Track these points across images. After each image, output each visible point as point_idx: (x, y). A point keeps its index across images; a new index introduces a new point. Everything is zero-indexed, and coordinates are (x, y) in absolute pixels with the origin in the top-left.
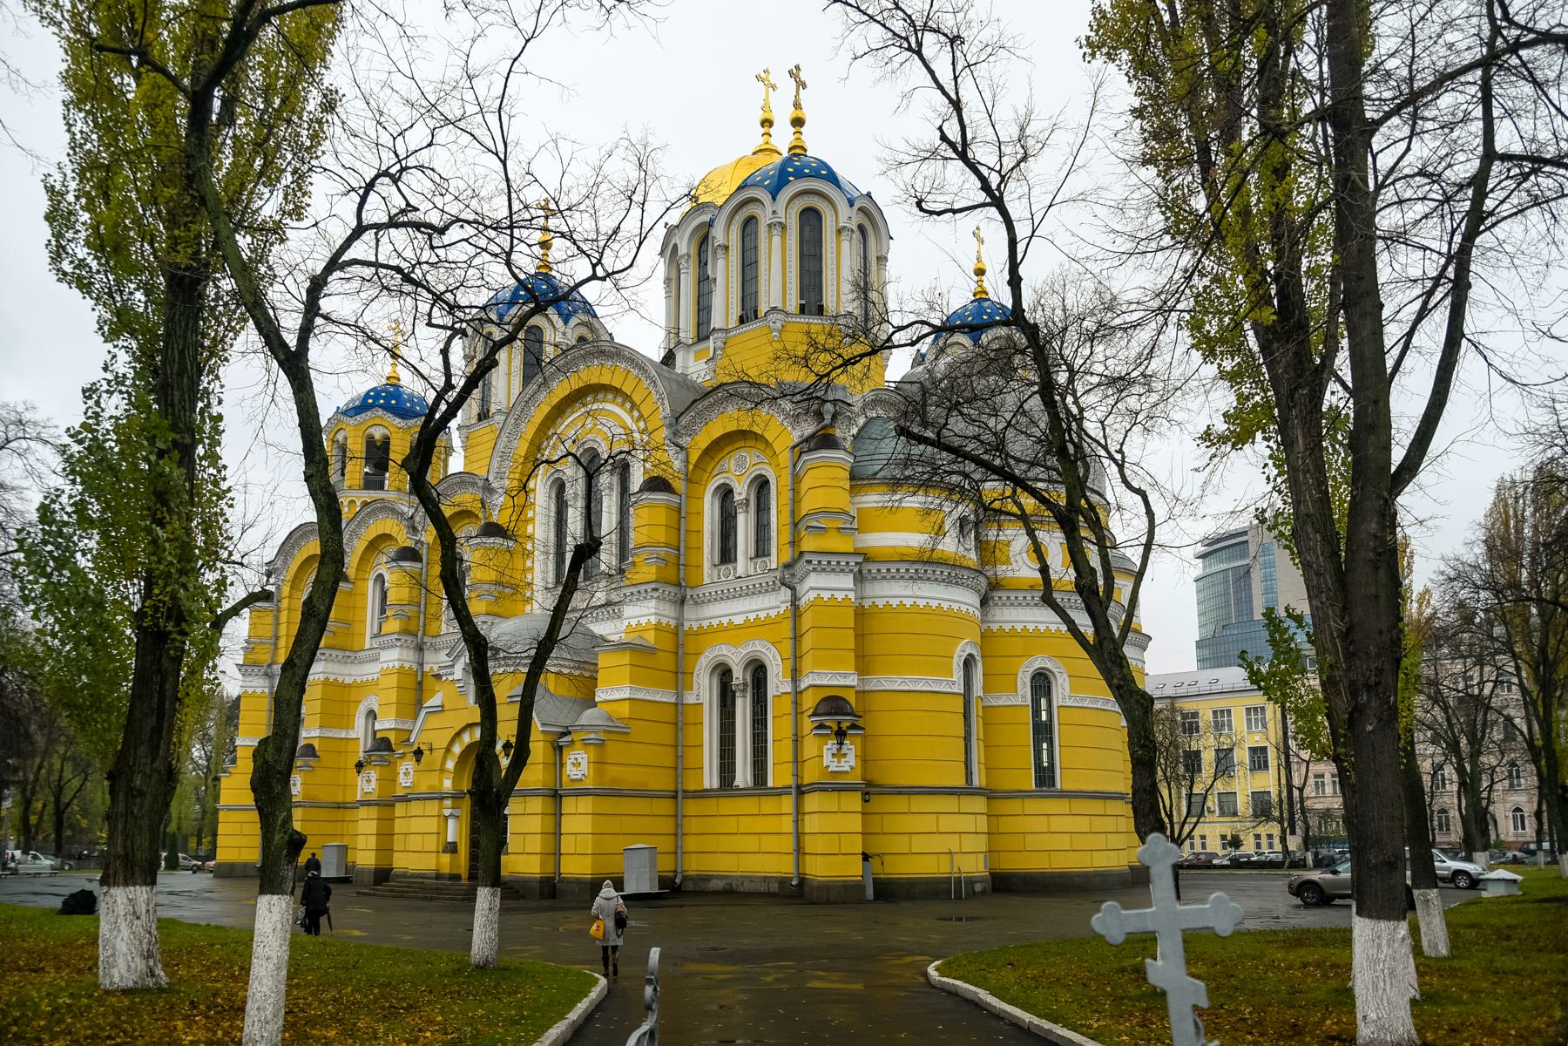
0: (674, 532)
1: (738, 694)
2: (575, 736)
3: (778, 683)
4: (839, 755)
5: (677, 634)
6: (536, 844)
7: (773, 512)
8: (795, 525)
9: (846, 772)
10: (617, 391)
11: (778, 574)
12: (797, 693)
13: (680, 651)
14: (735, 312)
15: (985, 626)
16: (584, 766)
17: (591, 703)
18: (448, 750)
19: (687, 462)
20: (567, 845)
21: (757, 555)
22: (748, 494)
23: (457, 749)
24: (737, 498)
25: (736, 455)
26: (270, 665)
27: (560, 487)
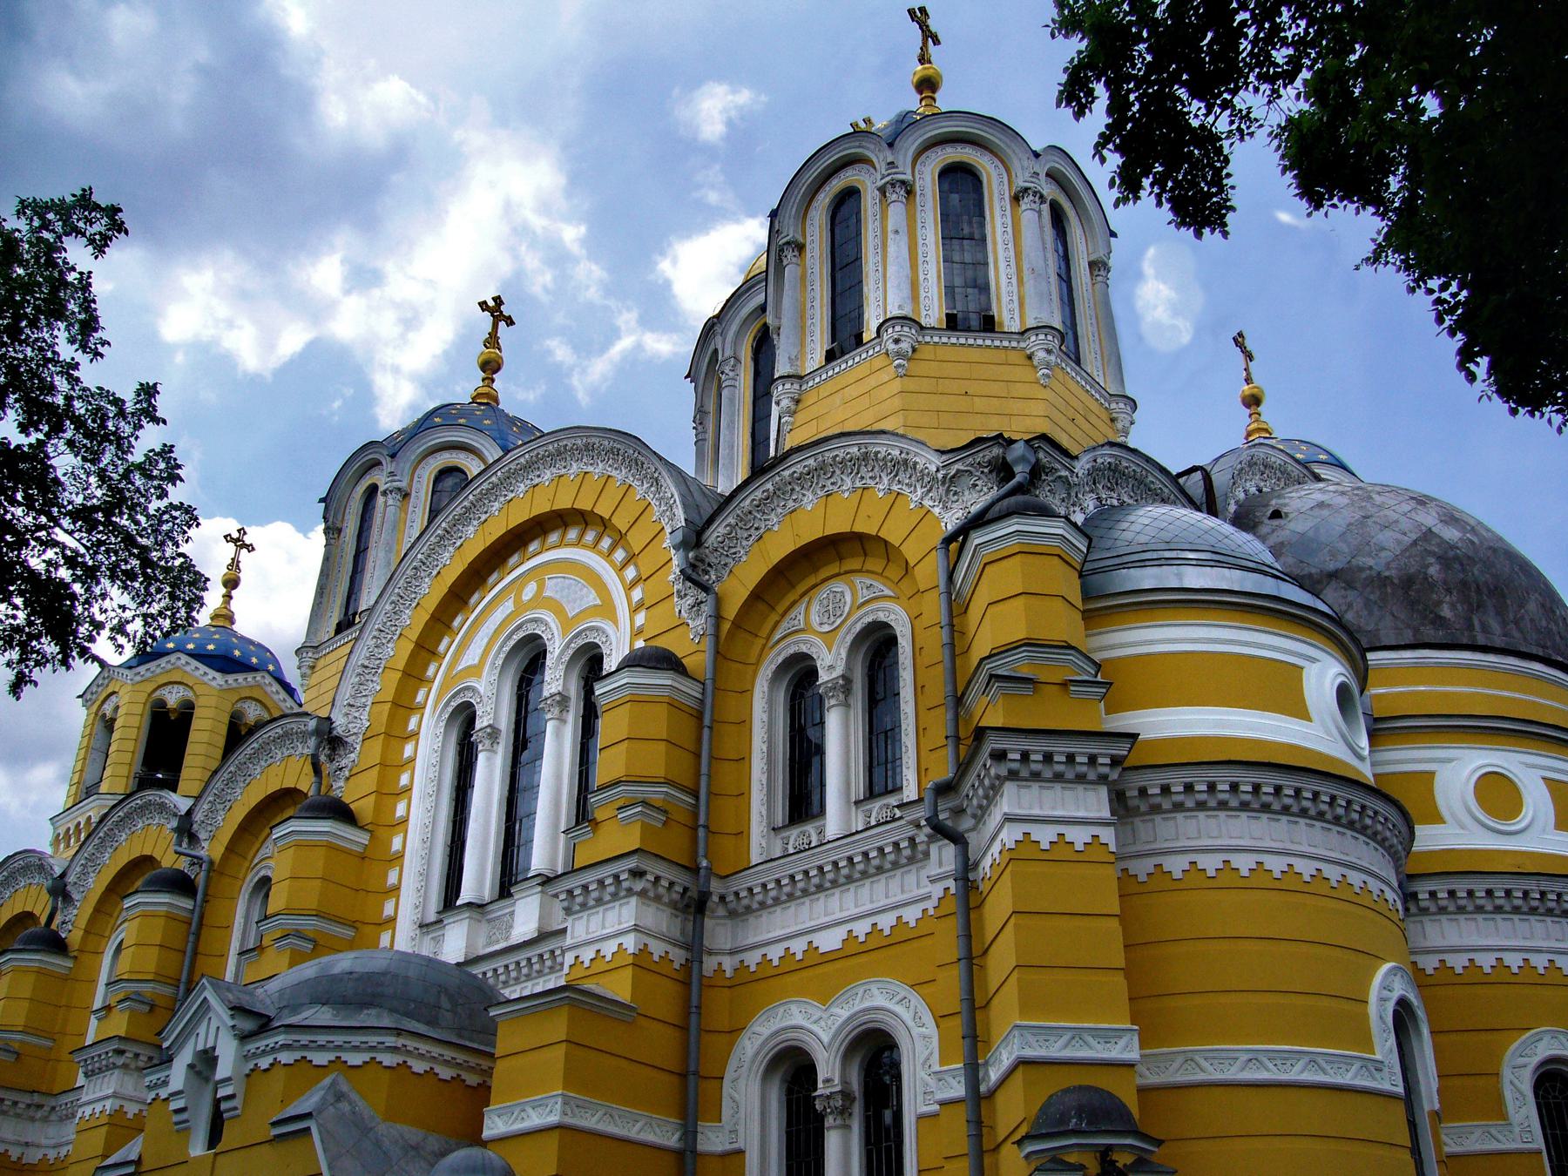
1: (829, 1121)
5: (686, 984)
11: (921, 813)
12: (978, 1101)
17: (473, 1136)
19: (718, 617)
21: (872, 793)
24: (823, 677)
25: (823, 593)
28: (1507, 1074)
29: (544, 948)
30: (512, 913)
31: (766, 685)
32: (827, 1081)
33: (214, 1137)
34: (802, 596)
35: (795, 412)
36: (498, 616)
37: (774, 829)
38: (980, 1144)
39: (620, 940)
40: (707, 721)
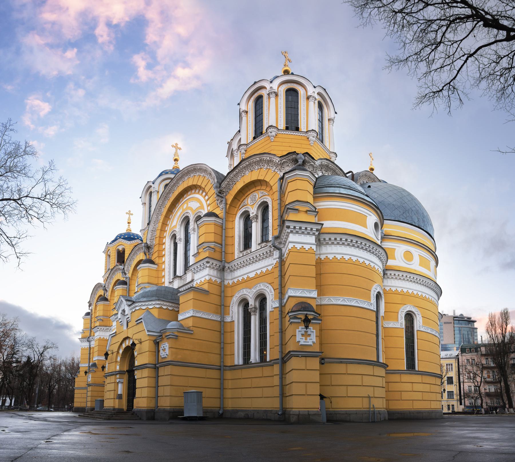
0: (219, 237)
3: (272, 304)
4: (306, 335)
12: (282, 307)
13: (222, 294)
19: (226, 204)
21: (262, 241)
22: (257, 213)
23: (121, 351)
24: (251, 215)
25: (251, 196)
32: (251, 305)
34: (246, 197)
35: (245, 153)
37: (240, 252)
38: (282, 316)
40: (224, 228)
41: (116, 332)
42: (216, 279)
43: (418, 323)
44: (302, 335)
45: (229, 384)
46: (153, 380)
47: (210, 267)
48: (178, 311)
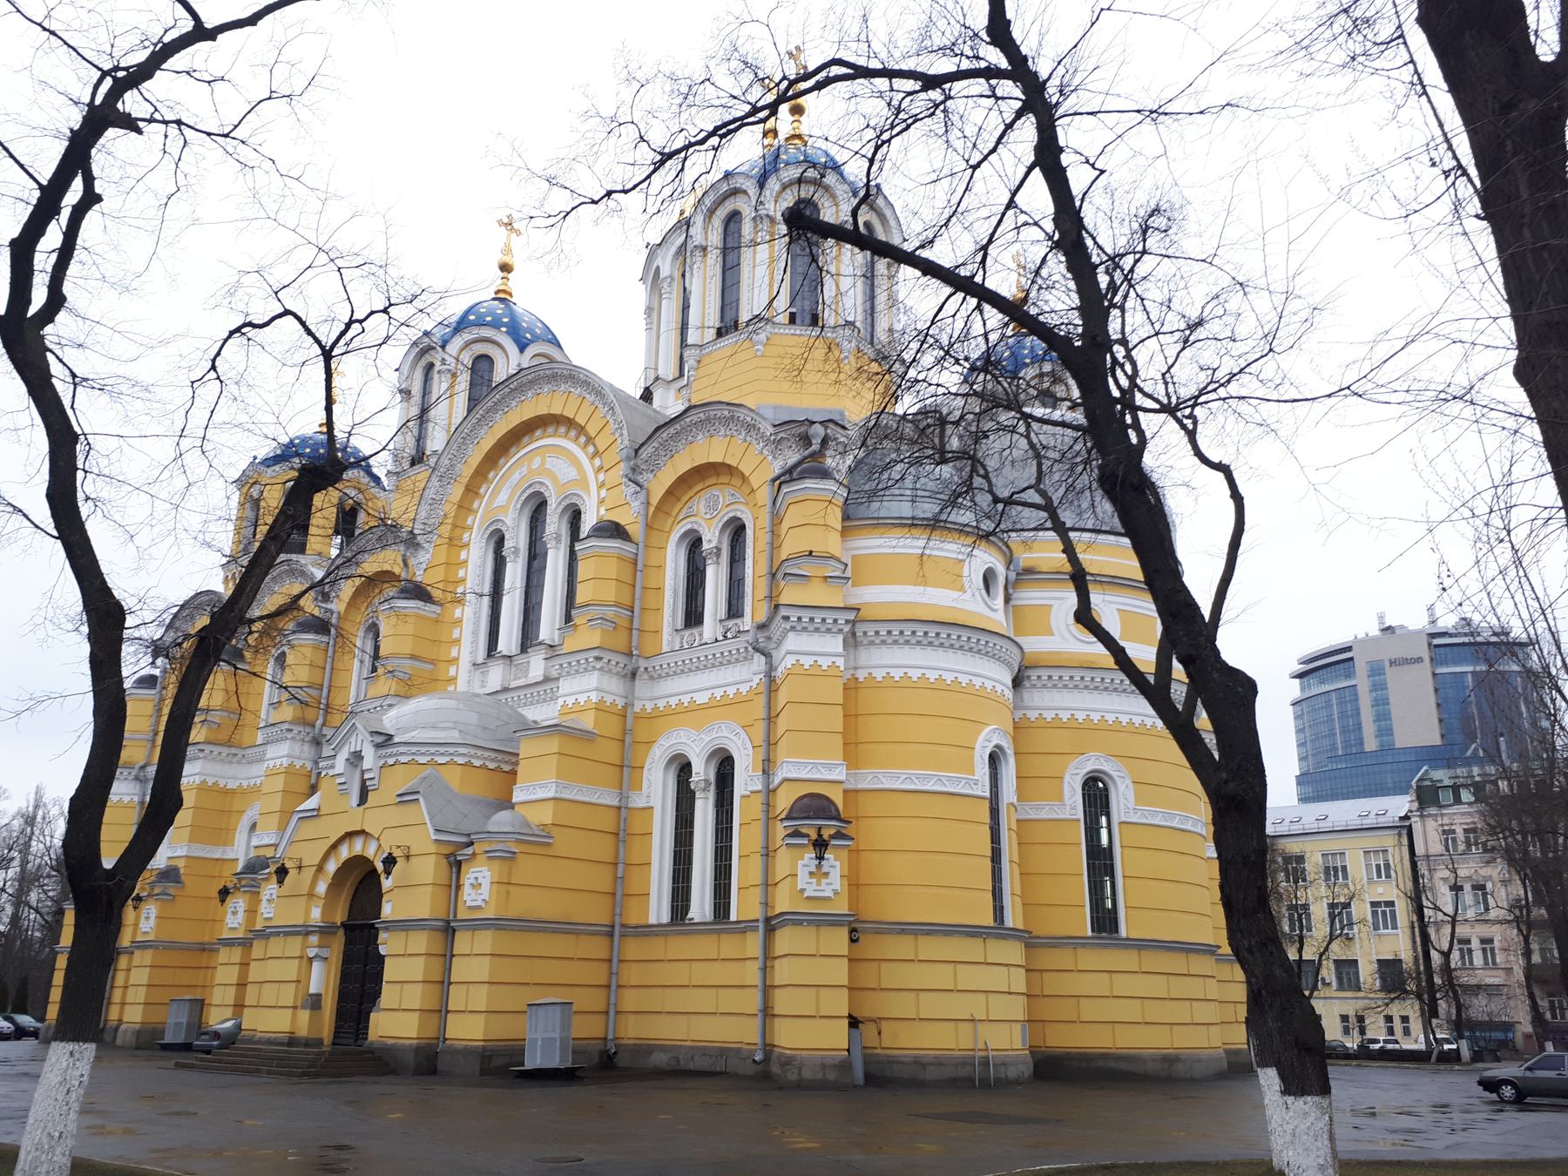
0: (627, 589)
2: (478, 848)
3: (745, 781)
4: (819, 874)
6: (415, 997)
7: (749, 562)
8: (774, 575)
9: (828, 899)
10: (569, 423)
11: (749, 637)
12: (770, 792)
13: (628, 738)
14: (713, 320)
15: (1019, 714)
16: (486, 884)
17: (506, 803)
18: (320, 868)
20: (456, 999)
22: (720, 542)
24: (705, 546)
25: (707, 494)
26: (143, 767)
27: (499, 541)
28: (1067, 778)
29: (547, 686)
30: (529, 662)
31: (674, 545)
33: (363, 798)
36: (517, 476)
38: (768, 815)
39: (588, 694)
41: (319, 810)
42: (615, 698)
43: (1122, 801)
44: (811, 874)
45: (632, 975)
46: (437, 964)
47: (601, 669)
48: (514, 773)
